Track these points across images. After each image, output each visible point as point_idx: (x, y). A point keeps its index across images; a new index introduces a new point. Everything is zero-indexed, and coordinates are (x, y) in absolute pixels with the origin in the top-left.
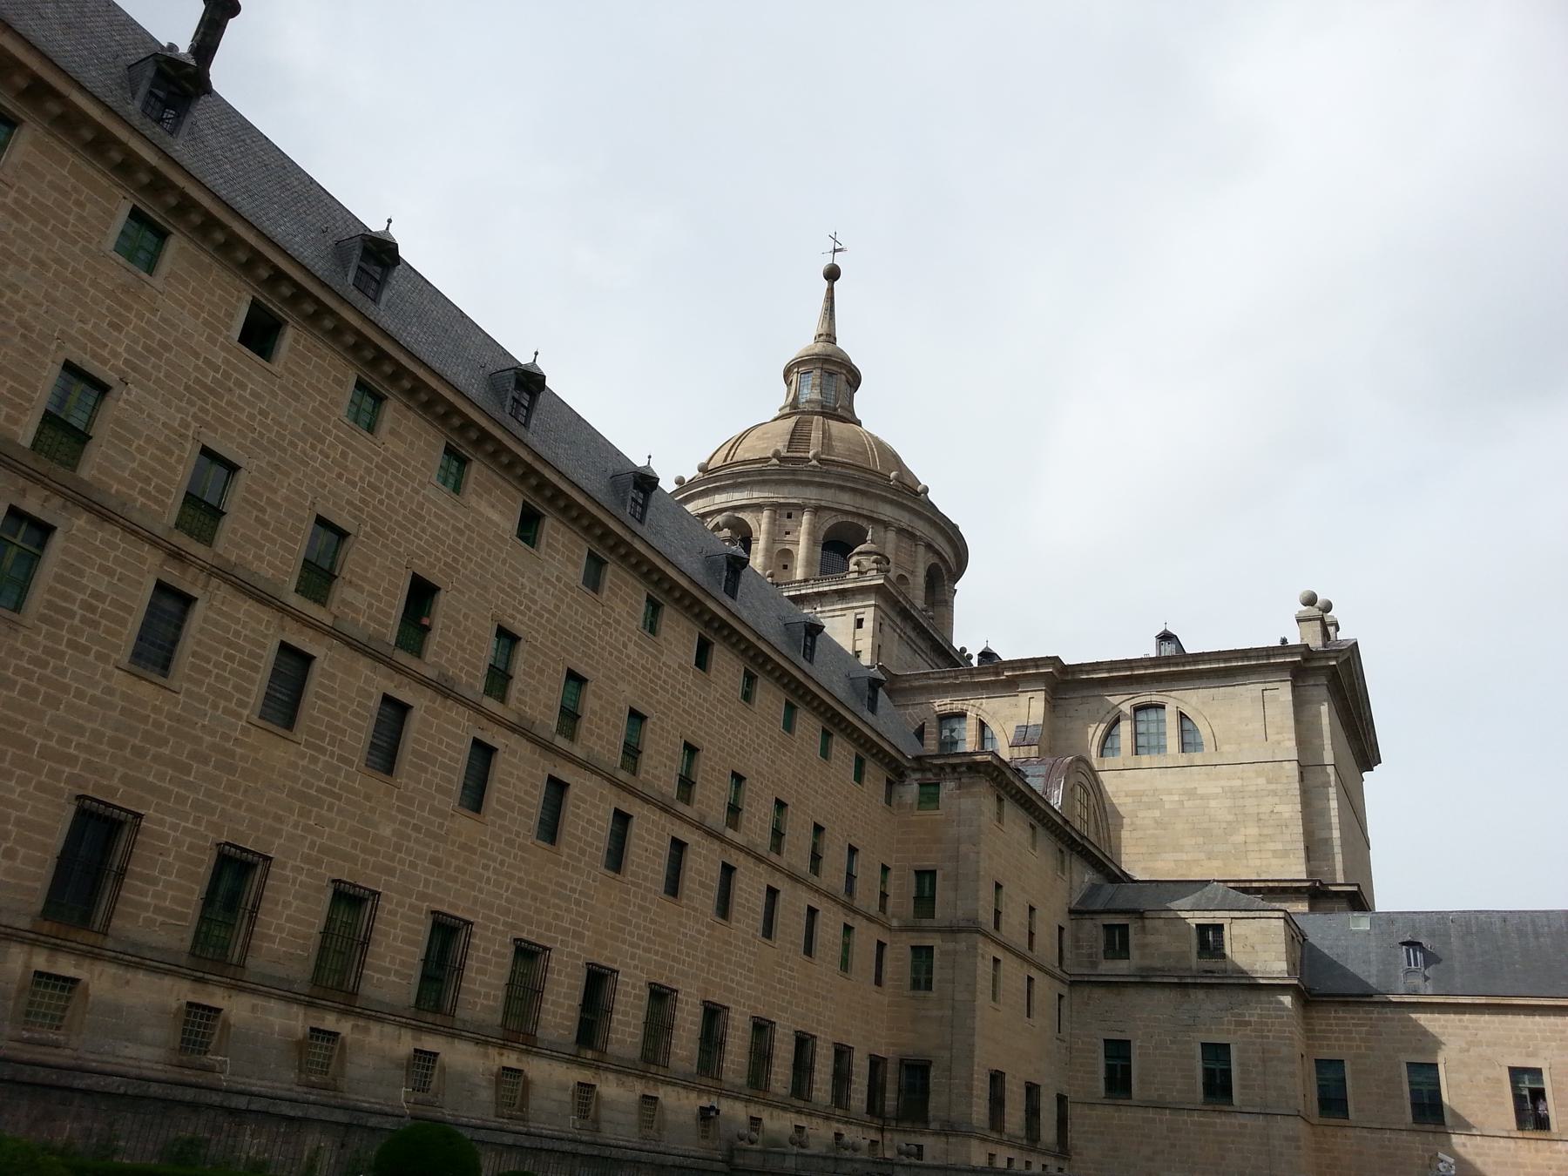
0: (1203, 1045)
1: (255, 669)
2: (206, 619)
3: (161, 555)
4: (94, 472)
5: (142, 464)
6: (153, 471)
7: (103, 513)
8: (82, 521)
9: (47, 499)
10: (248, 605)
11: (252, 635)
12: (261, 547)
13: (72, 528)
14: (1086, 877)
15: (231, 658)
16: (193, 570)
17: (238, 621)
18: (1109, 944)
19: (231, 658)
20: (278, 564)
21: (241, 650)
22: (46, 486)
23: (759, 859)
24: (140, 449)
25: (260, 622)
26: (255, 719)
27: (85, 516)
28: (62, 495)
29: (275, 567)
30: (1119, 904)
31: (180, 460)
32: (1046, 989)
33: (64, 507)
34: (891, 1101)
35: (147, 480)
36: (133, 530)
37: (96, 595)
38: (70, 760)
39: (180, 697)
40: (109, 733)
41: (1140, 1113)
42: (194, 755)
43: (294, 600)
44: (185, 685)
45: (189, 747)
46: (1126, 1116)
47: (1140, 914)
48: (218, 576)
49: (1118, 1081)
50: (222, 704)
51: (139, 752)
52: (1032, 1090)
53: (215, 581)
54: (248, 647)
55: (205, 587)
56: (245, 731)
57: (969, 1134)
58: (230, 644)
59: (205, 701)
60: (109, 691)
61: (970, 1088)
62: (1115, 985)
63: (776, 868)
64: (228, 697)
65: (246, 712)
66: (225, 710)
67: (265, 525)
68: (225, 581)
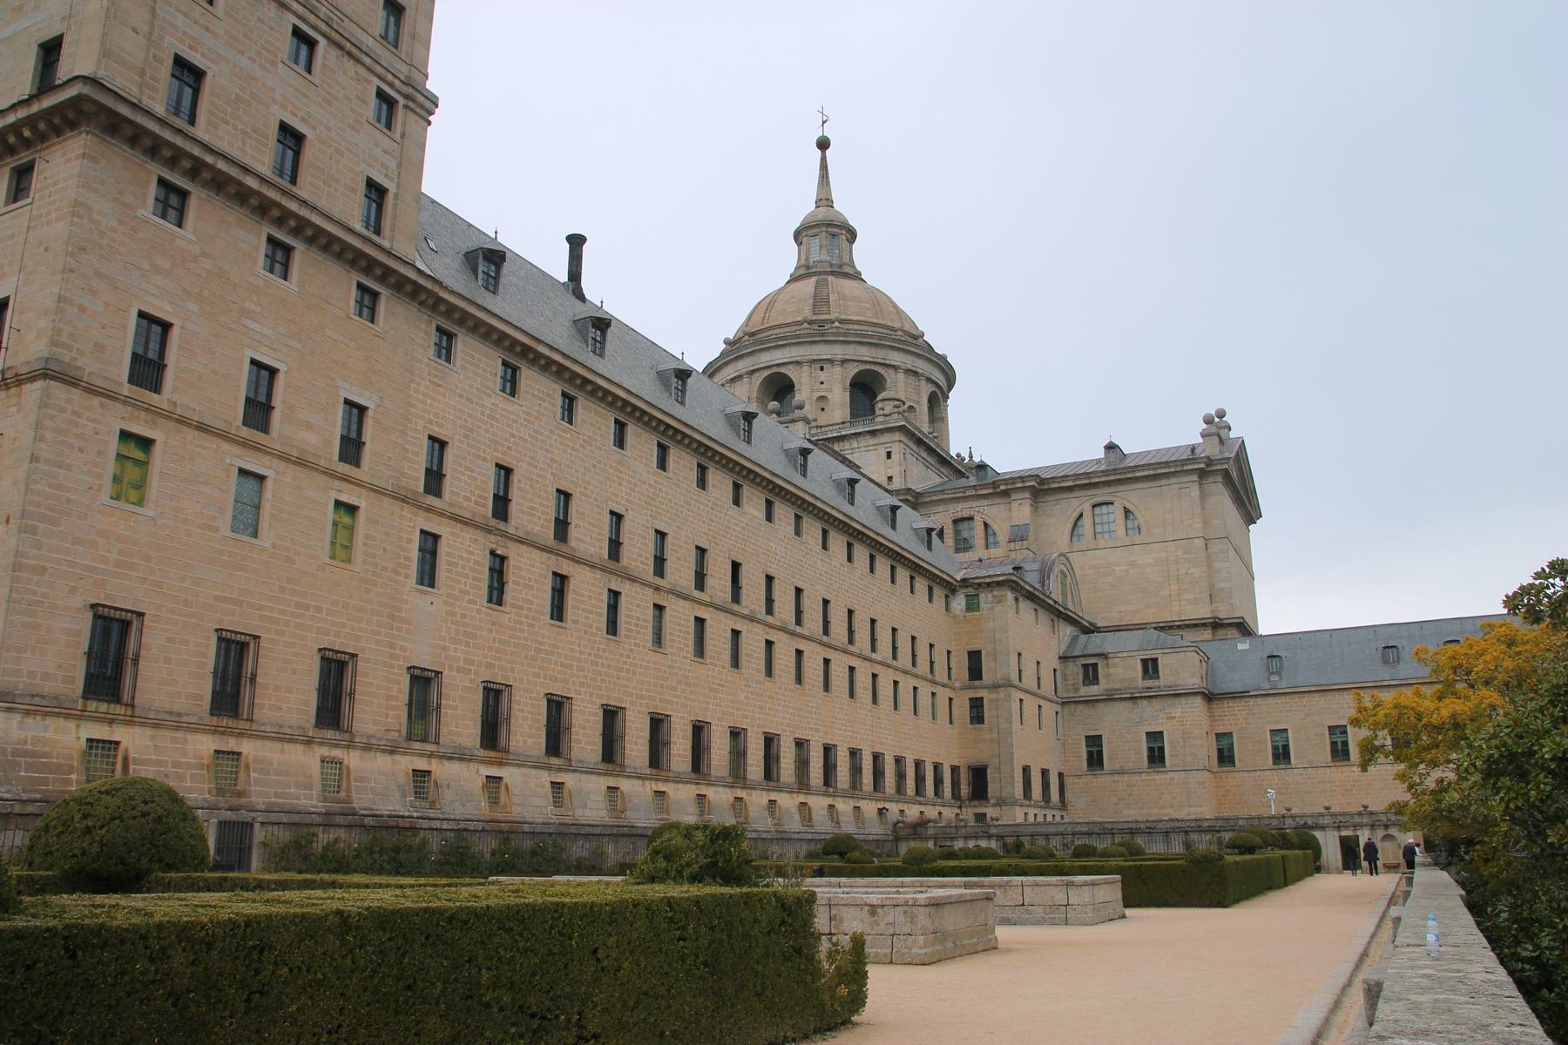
0: (1148, 734)
14: (1067, 631)
18: (1086, 675)
23: (888, 666)
30: (1091, 650)
32: (1049, 709)
34: (965, 790)
41: (1110, 778)
46: (1100, 780)
47: (1105, 656)
49: (1095, 760)
52: (1045, 773)
57: (1015, 803)
61: (1012, 777)
62: (1091, 702)
63: (896, 669)
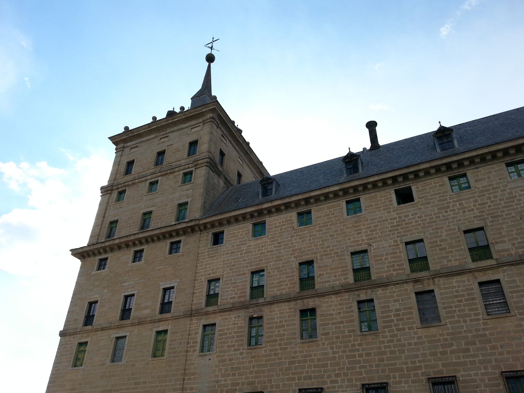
1: (474, 299)
2: (441, 294)
3: (411, 284)
4: (376, 275)
5: (389, 262)
6: (394, 262)
7: (384, 285)
8: (380, 291)
9: (366, 292)
10: (455, 280)
11: (465, 288)
12: (448, 257)
13: (379, 296)
15: (461, 301)
16: (426, 282)
17: (455, 287)
19: (461, 301)
20: (460, 257)
21: (463, 296)
22: (364, 289)
24: (386, 259)
25: (464, 282)
26: (486, 317)
27: (380, 289)
28: (369, 288)
29: (458, 260)
31: (400, 252)
33: (372, 291)
35: (394, 266)
36: (396, 283)
37: (397, 310)
38: (420, 367)
39: (449, 326)
40: (428, 352)
42: (467, 344)
43: (473, 265)
44: (447, 321)
45: (463, 342)
48: (436, 278)
50: (468, 319)
51: (443, 353)
53: (436, 280)
54: (465, 293)
55: (434, 283)
56: (484, 324)
58: (457, 297)
59: (460, 322)
60: (420, 338)
64: (468, 315)
65: (481, 316)
66: (471, 321)
67: (445, 249)
68: (440, 277)
